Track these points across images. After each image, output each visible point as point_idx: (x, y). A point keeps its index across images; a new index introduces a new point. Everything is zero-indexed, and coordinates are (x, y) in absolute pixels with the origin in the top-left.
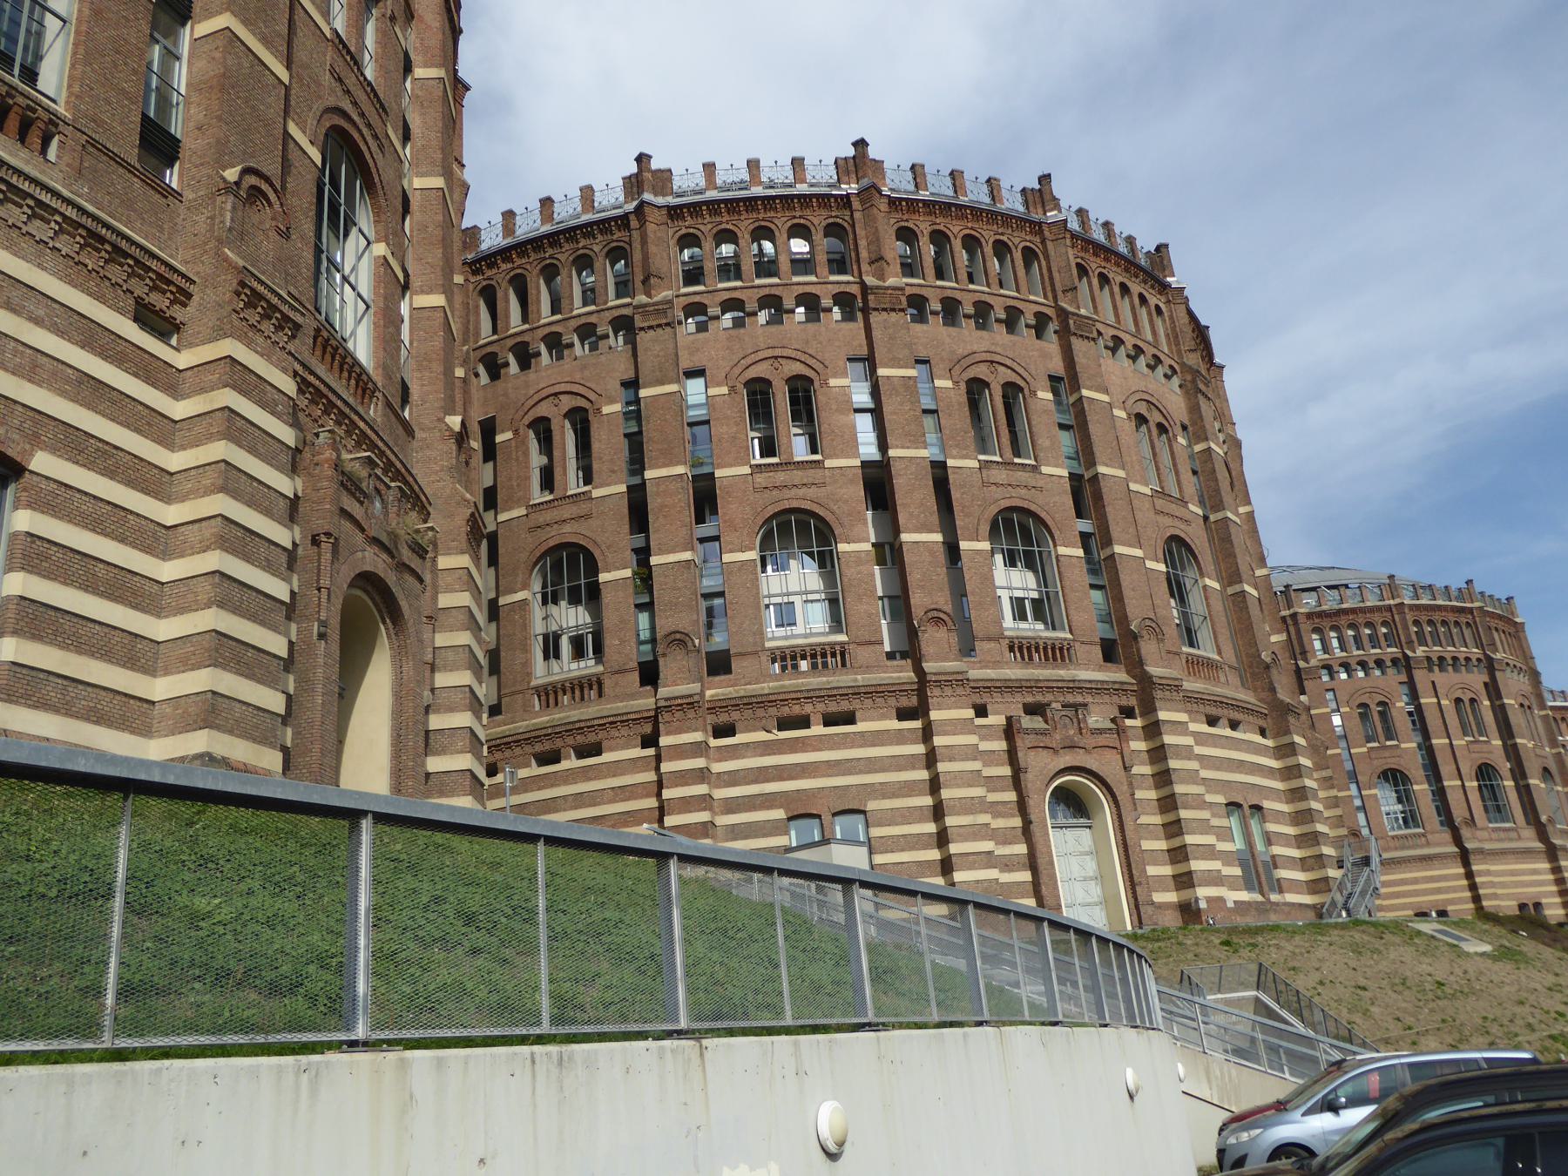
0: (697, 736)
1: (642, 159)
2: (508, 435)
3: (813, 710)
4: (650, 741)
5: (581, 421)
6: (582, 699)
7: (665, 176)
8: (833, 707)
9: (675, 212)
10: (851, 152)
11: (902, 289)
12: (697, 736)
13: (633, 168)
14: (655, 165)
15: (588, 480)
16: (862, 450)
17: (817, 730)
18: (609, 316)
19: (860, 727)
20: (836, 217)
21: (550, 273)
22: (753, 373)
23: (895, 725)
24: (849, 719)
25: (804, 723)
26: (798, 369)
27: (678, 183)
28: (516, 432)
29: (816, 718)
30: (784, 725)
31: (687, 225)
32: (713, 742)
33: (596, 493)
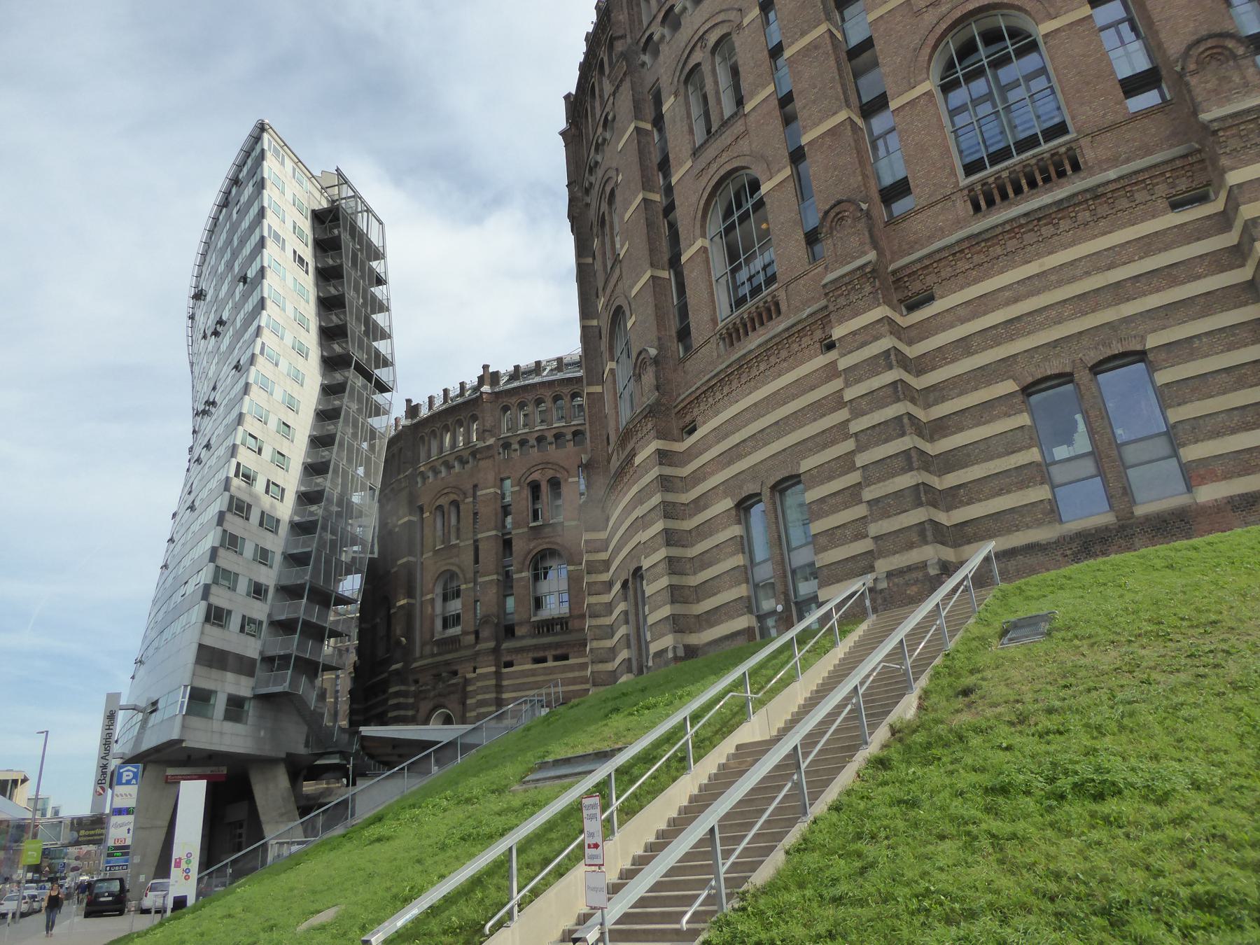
1: (486, 367)
4: (475, 669)
8: (559, 652)
15: (458, 538)
17: (550, 664)
19: (571, 661)
24: (565, 657)
25: (544, 660)
29: (550, 658)
33: (462, 544)
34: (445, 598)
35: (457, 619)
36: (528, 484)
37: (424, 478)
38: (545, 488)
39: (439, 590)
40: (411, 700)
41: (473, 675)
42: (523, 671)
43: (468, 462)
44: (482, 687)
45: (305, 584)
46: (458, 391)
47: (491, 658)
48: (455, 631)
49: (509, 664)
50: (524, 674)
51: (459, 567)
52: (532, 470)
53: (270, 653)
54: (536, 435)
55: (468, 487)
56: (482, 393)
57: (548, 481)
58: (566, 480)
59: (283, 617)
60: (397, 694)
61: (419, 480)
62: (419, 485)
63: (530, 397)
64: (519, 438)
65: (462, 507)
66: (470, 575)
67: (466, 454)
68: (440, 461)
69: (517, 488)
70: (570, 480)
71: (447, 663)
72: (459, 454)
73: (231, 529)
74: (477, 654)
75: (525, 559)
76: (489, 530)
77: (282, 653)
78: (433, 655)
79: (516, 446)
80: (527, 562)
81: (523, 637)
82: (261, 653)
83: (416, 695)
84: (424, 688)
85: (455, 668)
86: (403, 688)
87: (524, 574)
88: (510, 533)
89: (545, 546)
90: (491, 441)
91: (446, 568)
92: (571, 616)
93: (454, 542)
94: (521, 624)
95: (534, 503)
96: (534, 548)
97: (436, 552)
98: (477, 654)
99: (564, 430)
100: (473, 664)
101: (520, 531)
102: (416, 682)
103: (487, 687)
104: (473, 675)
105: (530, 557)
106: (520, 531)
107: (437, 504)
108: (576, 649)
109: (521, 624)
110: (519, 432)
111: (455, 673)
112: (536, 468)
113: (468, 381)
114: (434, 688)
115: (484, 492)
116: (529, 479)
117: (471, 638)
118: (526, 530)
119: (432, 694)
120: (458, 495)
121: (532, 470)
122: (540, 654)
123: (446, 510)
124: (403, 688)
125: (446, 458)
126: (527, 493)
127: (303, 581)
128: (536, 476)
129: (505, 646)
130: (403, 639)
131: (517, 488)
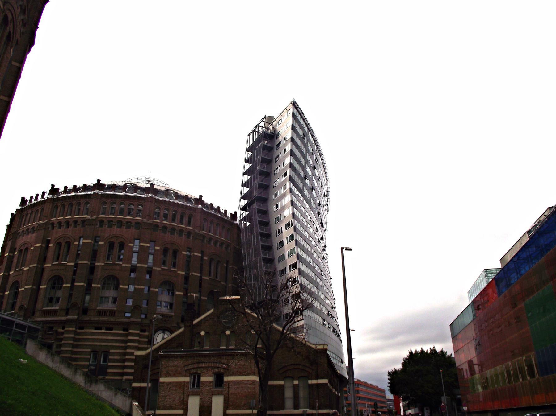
0: (138, 332)
1: (99, 181)
4: (63, 328)
6: (55, 315)
12: (138, 332)
14: (101, 182)
16: (133, 262)
17: (103, 331)
22: (112, 240)
23: (122, 332)
24: (111, 329)
26: (122, 240)
30: (96, 329)
32: (78, 331)
38: (117, 246)
41: (63, 331)
46: (63, 190)
104: (63, 331)
113: (69, 187)
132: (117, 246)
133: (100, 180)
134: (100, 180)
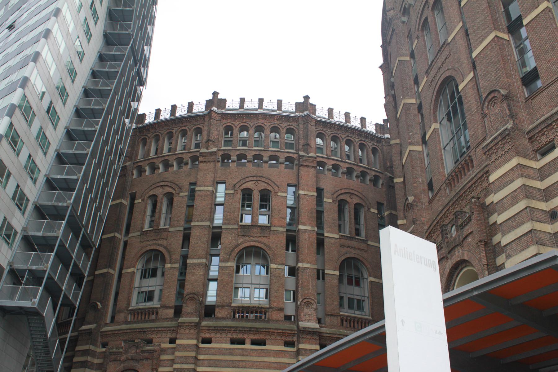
1: (215, 94)
2: (140, 201)
3: (248, 338)
4: (172, 341)
5: (170, 198)
7: (223, 102)
8: (256, 337)
9: (224, 116)
10: (302, 100)
11: (315, 158)
13: (210, 97)
14: (220, 97)
17: (248, 346)
18: (190, 155)
20: (291, 125)
21: (170, 136)
23: (283, 348)
24: (262, 343)
25: (242, 342)
27: (229, 105)
28: (143, 200)
29: (248, 341)
30: (233, 342)
31: (229, 122)
32: (202, 346)
34: (144, 276)
35: (149, 297)
36: (242, 190)
37: (141, 171)
38: (256, 196)
39: (139, 266)
40: (96, 361)
42: (220, 349)
43: (187, 164)
44: (181, 357)
45: (68, 207)
47: (192, 331)
48: (155, 304)
49: (208, 341)
50: (221, 351)
51: (165, 248)
52: (247, 180)
53: (18, 266)
54: (254, 153)
55: (185, 183)
56: (211, 111)
57: (260, 191)
58: (276, 193)
59: (40, 234)
60: (86, 353)
61: (135, 172)
62: (134, 177)
63: (252, 124)
64: (238, 153)
65: (176, 199)
66: (177, 256)
67: (186, 157)
68: (161, 159)
69: (232, 192)
70: (280, 194)
71: (143, 331)
72: (180, 156)
73: (16, 126)
74: (180, 326)
75: (232, 251)
76: (202, 220)
77: (34, 268)
78: (127, 323)
79: (235, 158)
80: (234, 254)
81: (223, 319)
82: (10, 264)
83: (104, 355)
84: (114, 350)
85: (149, 336)
86: (92, 348)
87: (229, 264)
88: (220, 228)
89: (252, 244)
90: (214, 149)
91: (153, 247)
92: (269, 308)
93: (162, 226)
94: (222, 307)
95: (242, 210)
96: (242, 243)
97: (144, 233)
98: (180, 326)
99: (277, 154)
100: (169, 335)
101: (231, 227)
102: (104, 345)
103: (187, 357)
105: (237, 250)
106: (231, 227)
107: (151, 193)
108: (273, 337)
109: (222, 307)
110: (238, 148)
111: (150, 342)
112: (250, 179)
114: (126, 352)
115: (202, 188)
116: (244, 187)
117: (171, 312)
118: (236, 227)
119: (123, 358)
120: (174, 189)
121: (247, 180)
122: (240, 336)
123: (159, 200)
124: (92, 348)
125: (167, 158)
126: (239, 196)
127: (65, 204)
128: (250, 185)
129: (204, 323)
130: (99, 304)
131: (232, 192)
132: (256, 196)
133: (218, 93)
134: (218, 93)
